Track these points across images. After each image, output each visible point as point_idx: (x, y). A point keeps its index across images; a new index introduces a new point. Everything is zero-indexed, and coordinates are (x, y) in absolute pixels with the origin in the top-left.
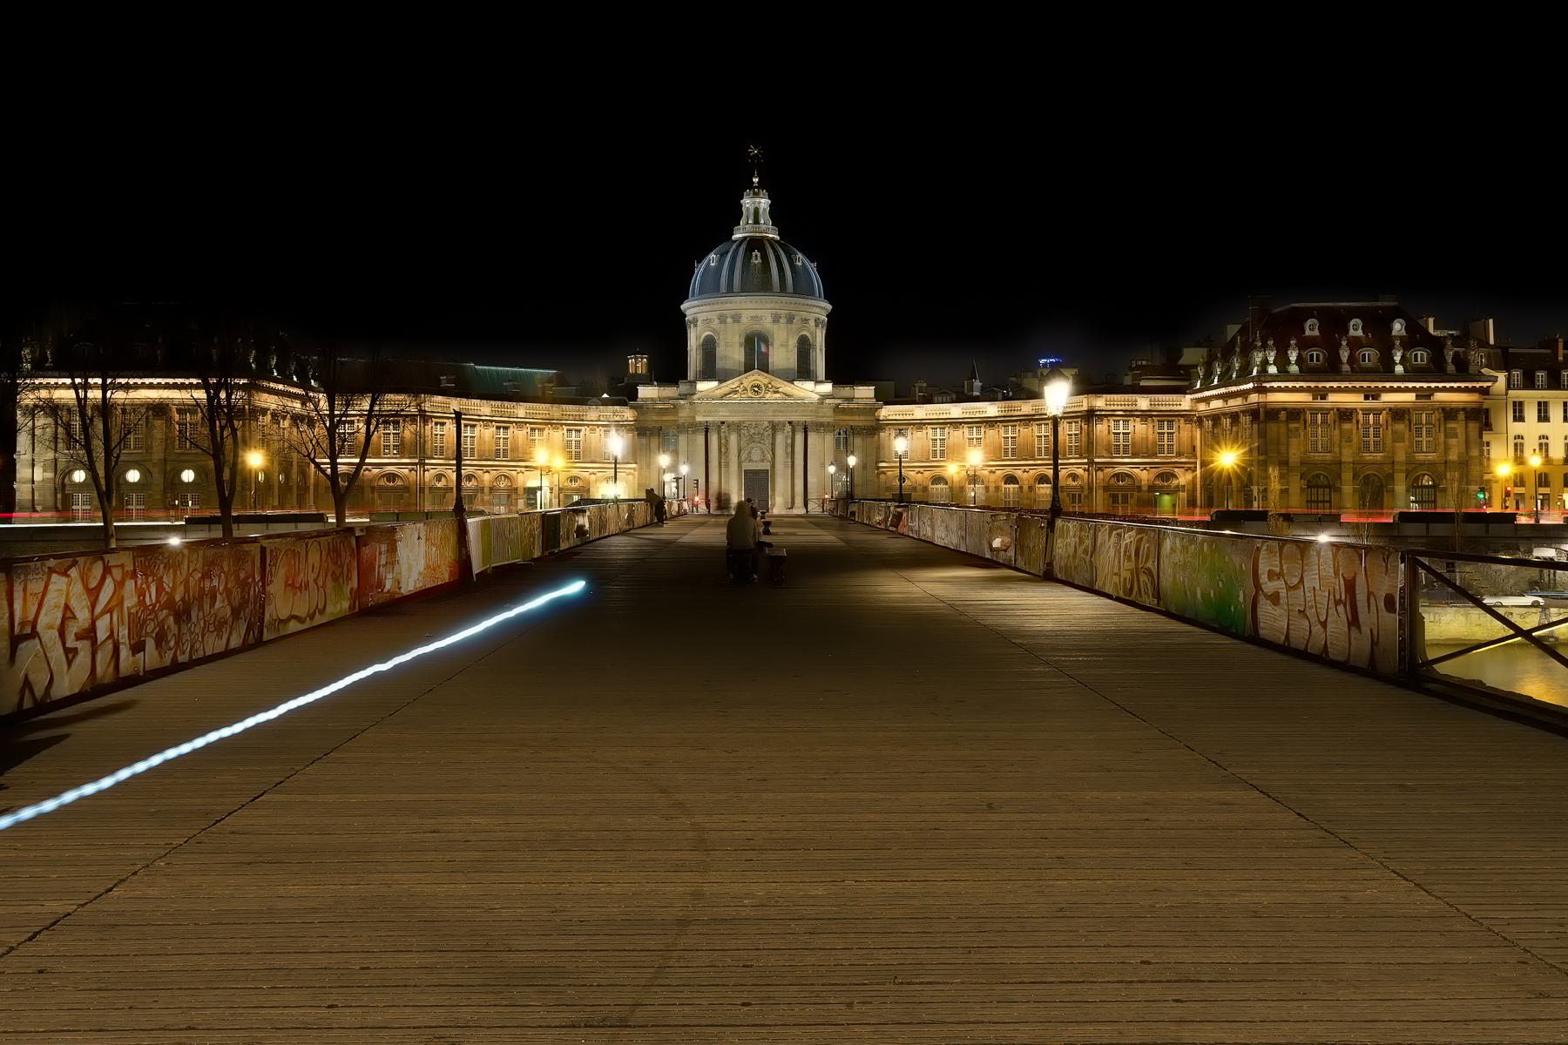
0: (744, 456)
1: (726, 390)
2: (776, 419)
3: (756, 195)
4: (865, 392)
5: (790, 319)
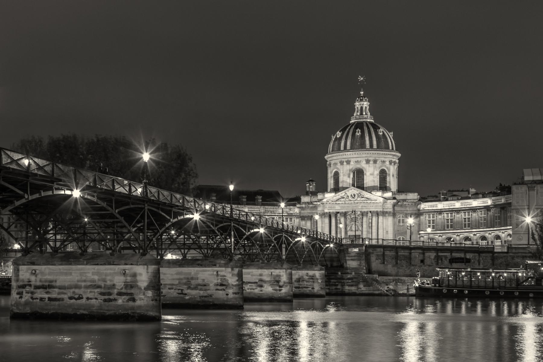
0: (348, 228)
1: (339, 197)
2: (363, 210)
3: (361, 100)
4: (413, 196)
5: (375, 162)
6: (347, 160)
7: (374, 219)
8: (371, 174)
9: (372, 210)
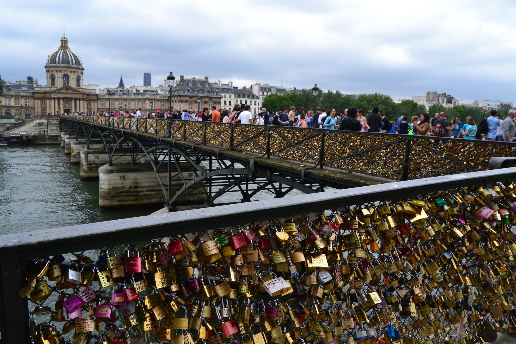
7: (78, 102)
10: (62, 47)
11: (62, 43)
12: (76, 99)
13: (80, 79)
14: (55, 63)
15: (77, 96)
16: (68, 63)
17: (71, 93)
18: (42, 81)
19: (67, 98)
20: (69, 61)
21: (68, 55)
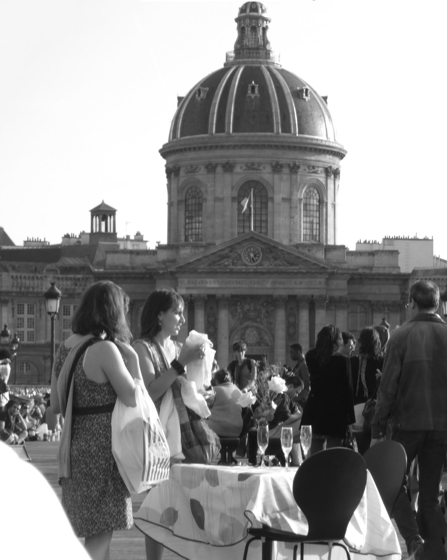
6: (224, 160)
7: (304, 315)
8: (284, 199)
9: (297, 292)
10: (241, 48)
11: (241, 30)
12: (293, 302)
13: (322, 203)
14: (205, 129)
15: (300, 287)
16: (268, 126)
17: (269, 273)
18: (146, 218)
19: (254, 298)
20: (269, 117)
21: (264, 89)
